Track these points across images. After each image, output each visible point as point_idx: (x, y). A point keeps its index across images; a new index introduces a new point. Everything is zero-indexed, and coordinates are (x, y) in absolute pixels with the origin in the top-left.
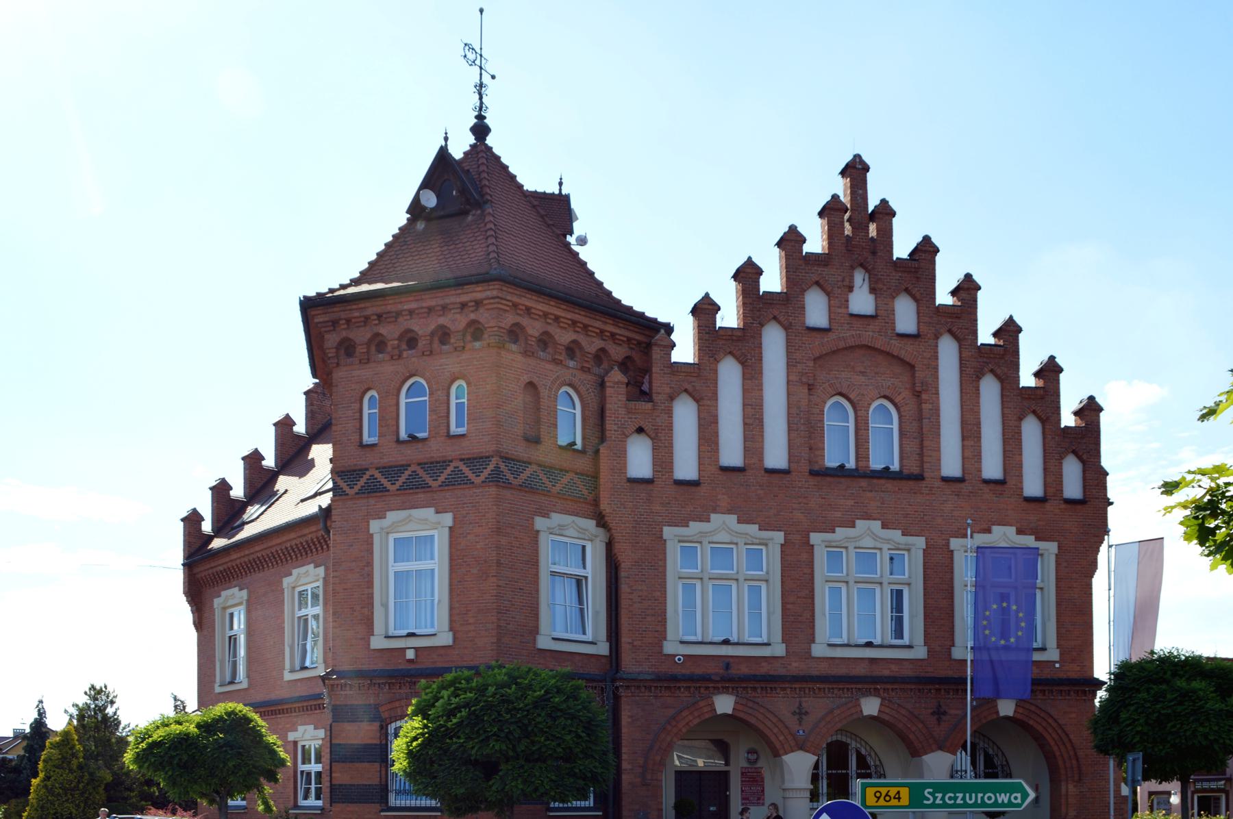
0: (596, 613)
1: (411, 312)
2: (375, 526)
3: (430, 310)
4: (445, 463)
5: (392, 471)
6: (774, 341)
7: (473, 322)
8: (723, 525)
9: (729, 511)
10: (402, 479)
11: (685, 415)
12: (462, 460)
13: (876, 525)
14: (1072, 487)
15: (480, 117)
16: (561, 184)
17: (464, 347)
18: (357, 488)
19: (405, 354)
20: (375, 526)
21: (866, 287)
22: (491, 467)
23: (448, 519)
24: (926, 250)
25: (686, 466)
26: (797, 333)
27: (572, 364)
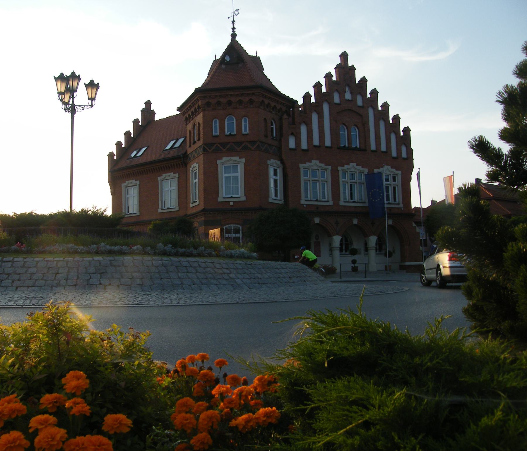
0: (280, 191)
1: (231, 95)
2: (219, 162)
3: (238, 95)
4: (242, 143)
5: (224, 144)
6: (326, 108)
7: (251, 99)
8: (315, 164)
9: (316, 159)
10: (227, 147)
11: (303, 129)
12: (247, 142)
13: (355, 164)
14: (404, 155)
15: (234, 31)
16: (257, 53)
17: (247, 107)
18: (212, 149)
19: (228, 108)
20: (219, 162)
21: (349, 91)
22: (257, 145)
23: (243, 160)
24: (364, 80)
25: (304, 145)
26: (332, 105)
27: (274, 112)
